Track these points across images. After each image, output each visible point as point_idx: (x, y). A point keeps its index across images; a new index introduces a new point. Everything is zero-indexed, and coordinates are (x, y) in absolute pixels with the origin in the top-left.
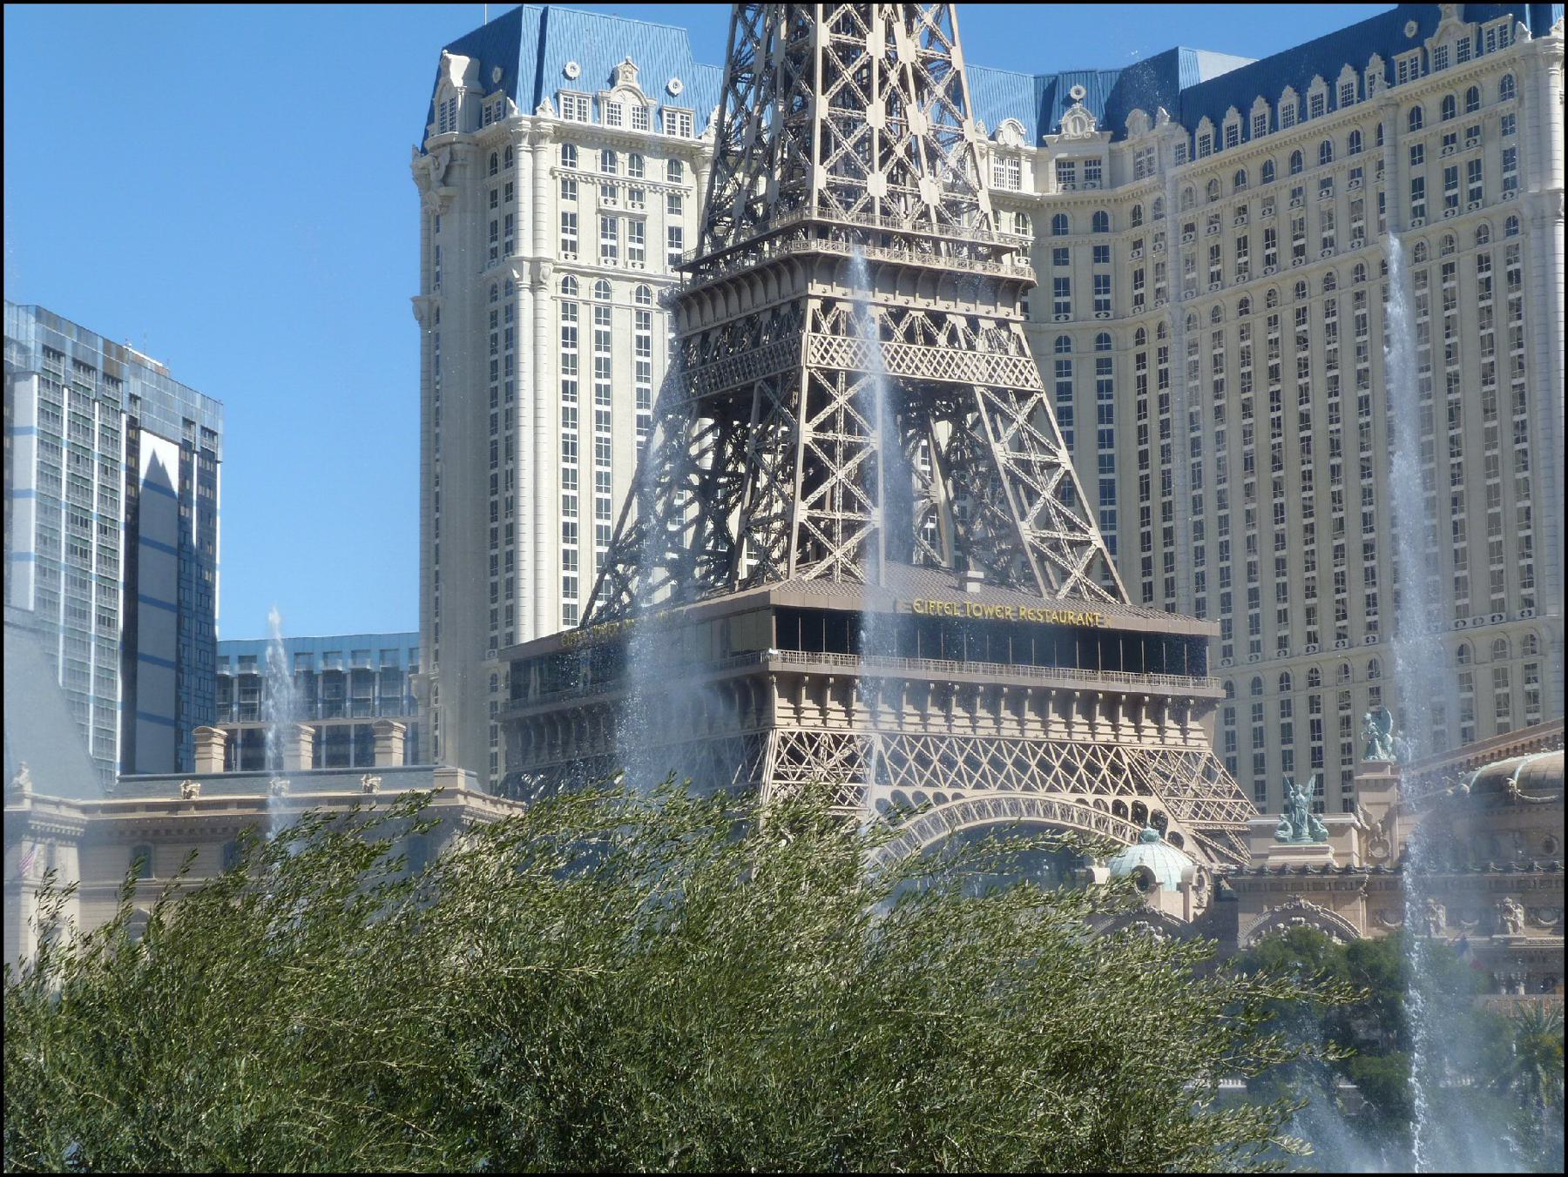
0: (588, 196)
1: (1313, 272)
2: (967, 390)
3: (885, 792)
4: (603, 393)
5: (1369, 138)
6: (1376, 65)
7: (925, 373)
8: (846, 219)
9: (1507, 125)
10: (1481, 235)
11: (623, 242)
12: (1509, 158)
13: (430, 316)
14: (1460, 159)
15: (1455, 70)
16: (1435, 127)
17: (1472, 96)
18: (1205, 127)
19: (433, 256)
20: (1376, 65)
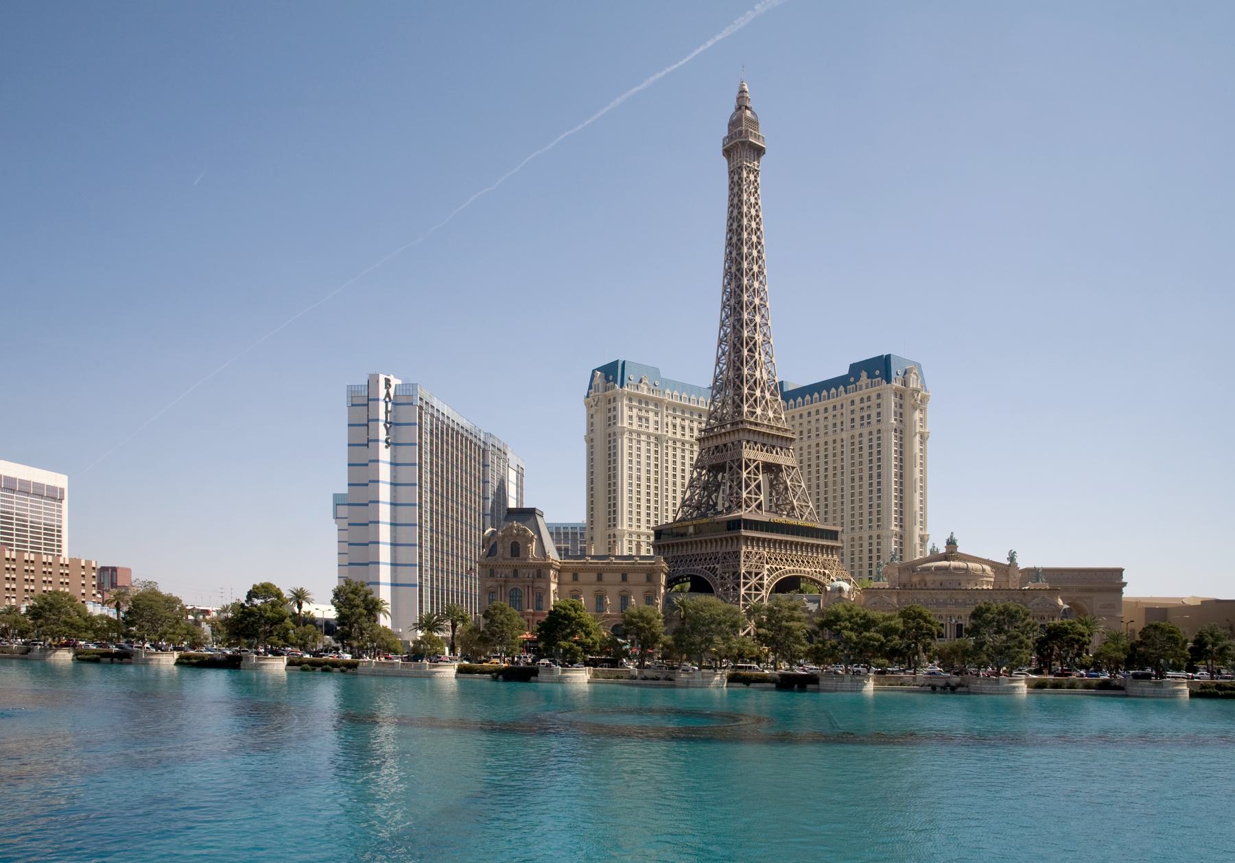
0: (635, 411)
1: (821, 441)
2: (780, 466)
3: (767, 566)
4: (639, 463)
5: (839, 407)
6: (841, 388)
7: (771, 461)
8: (752, 420)
9: (879, 406)
10: (871, 433)
11: (644, 424)
12: (879, 414)
13: (590, 441)
14: (865, 414)
15: (865, 391)
16: (858, 405)
17: (869, 398)
18: (792, 402)
19: (591, 425)
20: (841, 388)
